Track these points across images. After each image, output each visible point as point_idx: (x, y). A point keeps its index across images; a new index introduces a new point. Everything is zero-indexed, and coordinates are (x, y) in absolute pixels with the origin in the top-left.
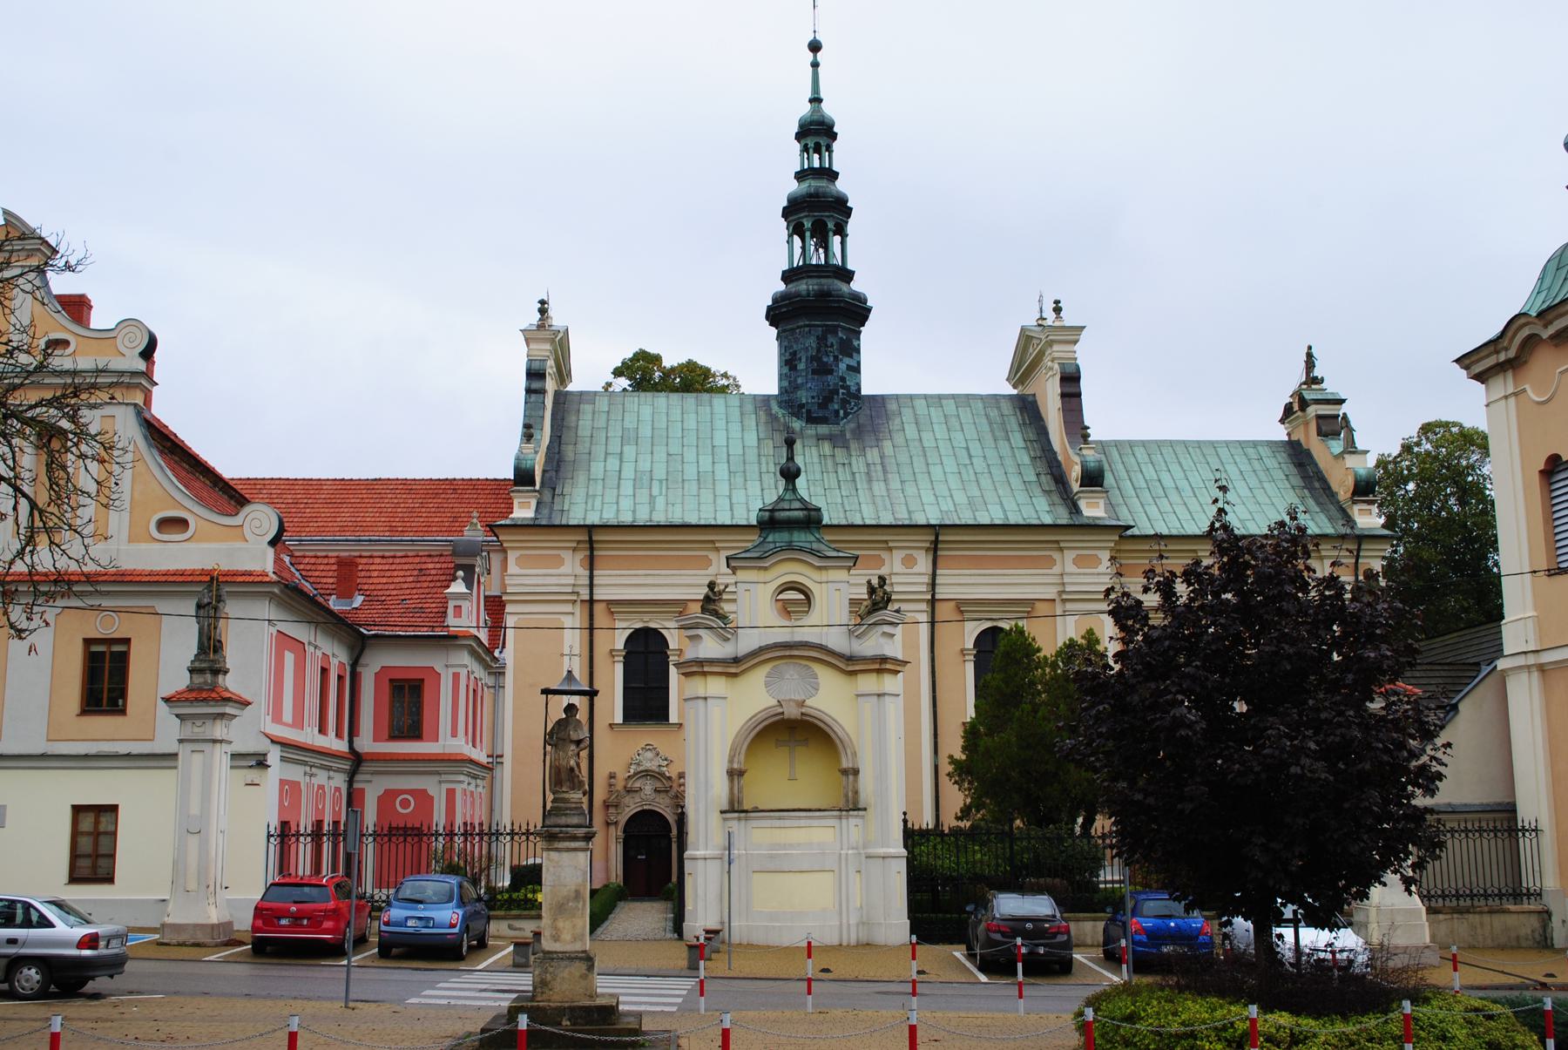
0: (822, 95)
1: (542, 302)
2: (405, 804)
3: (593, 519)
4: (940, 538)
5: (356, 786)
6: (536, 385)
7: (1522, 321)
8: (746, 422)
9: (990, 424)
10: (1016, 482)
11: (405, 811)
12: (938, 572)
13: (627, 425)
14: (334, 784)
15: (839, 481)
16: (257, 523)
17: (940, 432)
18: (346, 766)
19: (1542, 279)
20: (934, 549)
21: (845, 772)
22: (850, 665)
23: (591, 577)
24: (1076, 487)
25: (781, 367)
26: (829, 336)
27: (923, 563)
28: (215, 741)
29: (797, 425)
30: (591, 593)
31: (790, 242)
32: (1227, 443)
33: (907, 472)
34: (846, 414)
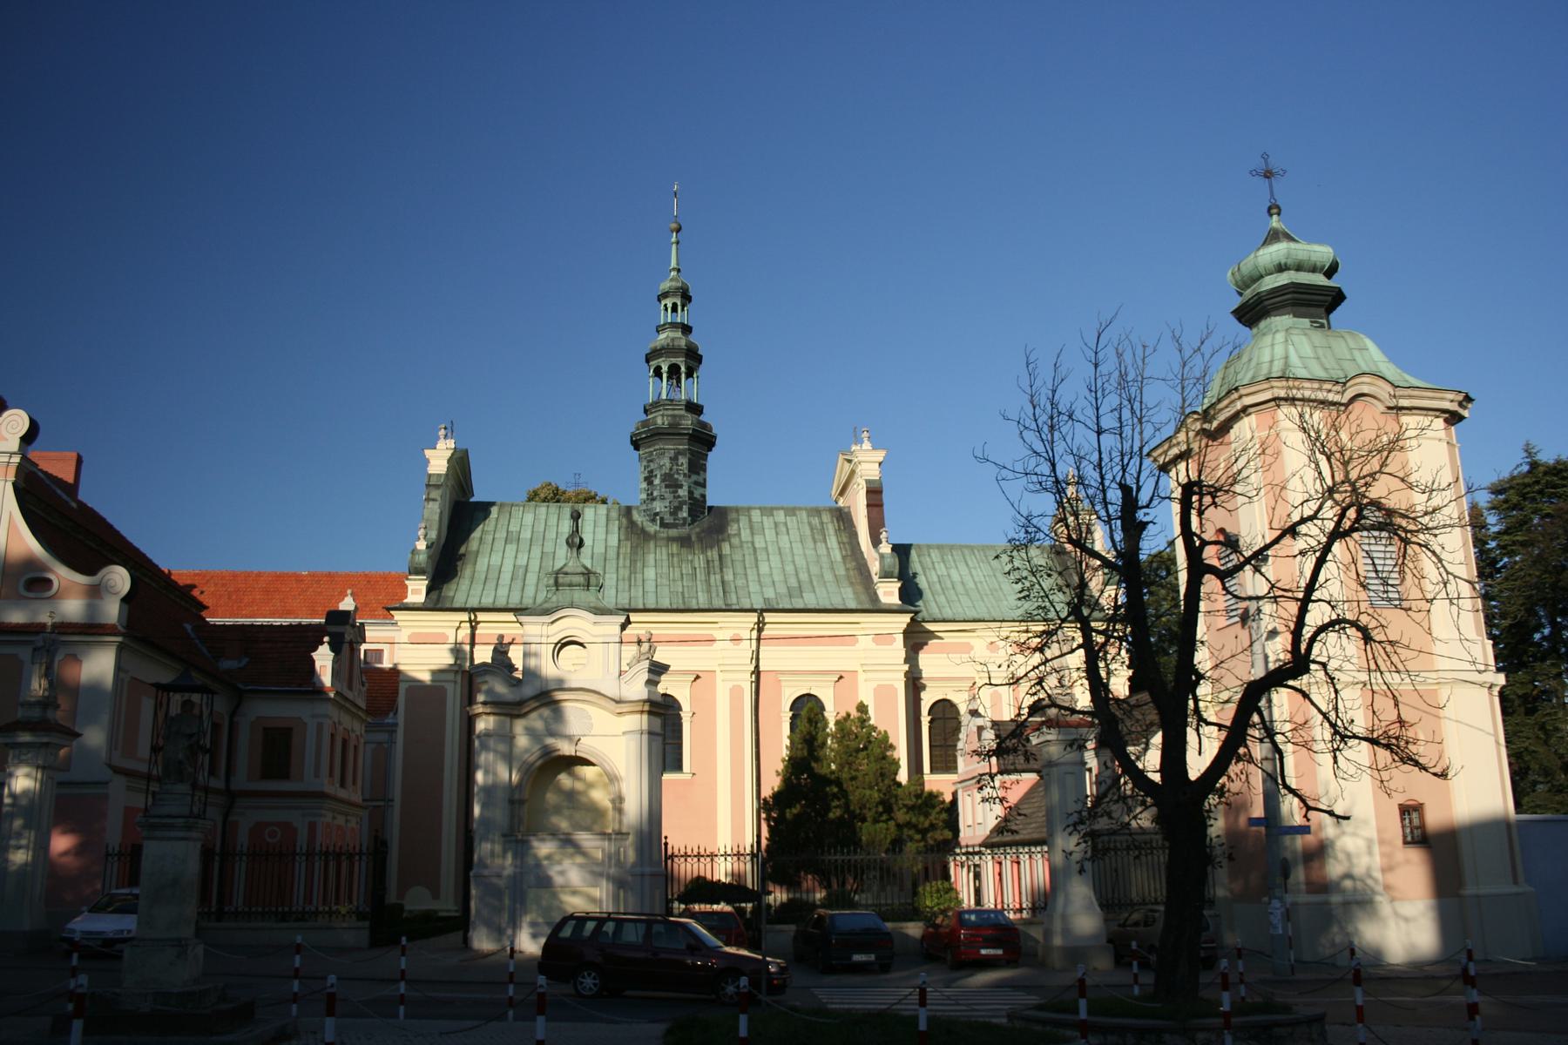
3: (473, 603)
9: (812, 529)
10: (828, 576)
13: (512, 528)
15: (682, 575)
24: (876, 579)
26: (680, 457)
29: (652, 528)
34: (693, 522)
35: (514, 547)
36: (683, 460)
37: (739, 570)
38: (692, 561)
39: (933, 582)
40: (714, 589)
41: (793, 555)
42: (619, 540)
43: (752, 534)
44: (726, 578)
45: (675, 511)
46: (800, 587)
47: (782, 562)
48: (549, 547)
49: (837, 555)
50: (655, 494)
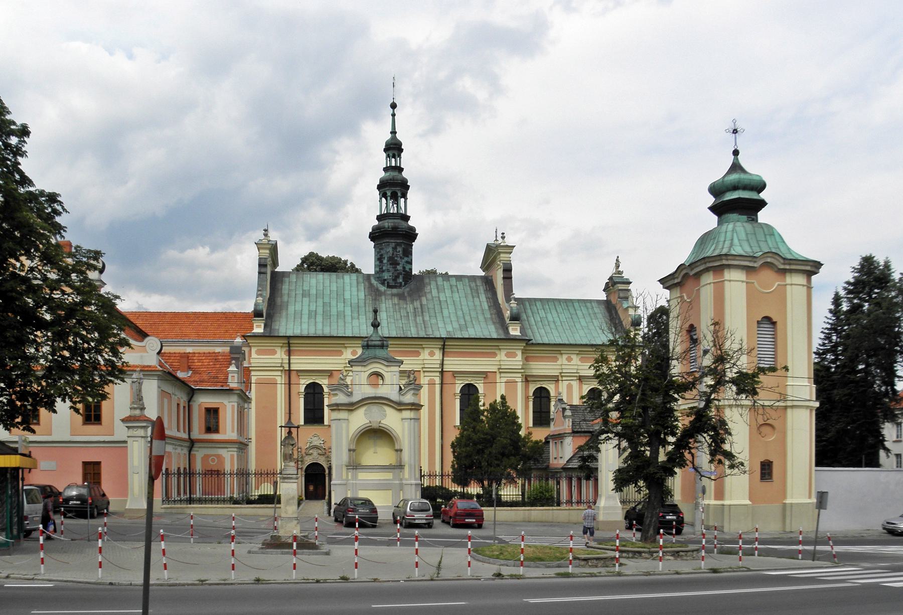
0: (397, 130)
1: (266, 230)
2: (213, 460)
4: (446, 343)
5: (192, 453)
8: (359, 287)
9: (471, 289)
10: (481, 318)
11: (213, 465)
12: (445, 359)
13: (305, 288)
14: (183, 452)
18: (187, 444)
20: (443, 348)
21: (397, 451)
22: (399, 406)
23: (289, 359)
24: (508, 321)
25: (375, 261)
27: (438, 355)
29: (382, 288)
30: (289, 367)
31: (380, 201)
33: (432, 311)
34: (405, 284)
36: (399, 249)
37: (432, 314)
38: (406, 308)
39: (538, 321)
41: (461, 305)
42: (365, 296)
43: (438, 293)
44: (425, 319)
45: (395, 280)
46: (466, 324)
47: (455, 309)
48: (327, 300)
50: (384, 268)
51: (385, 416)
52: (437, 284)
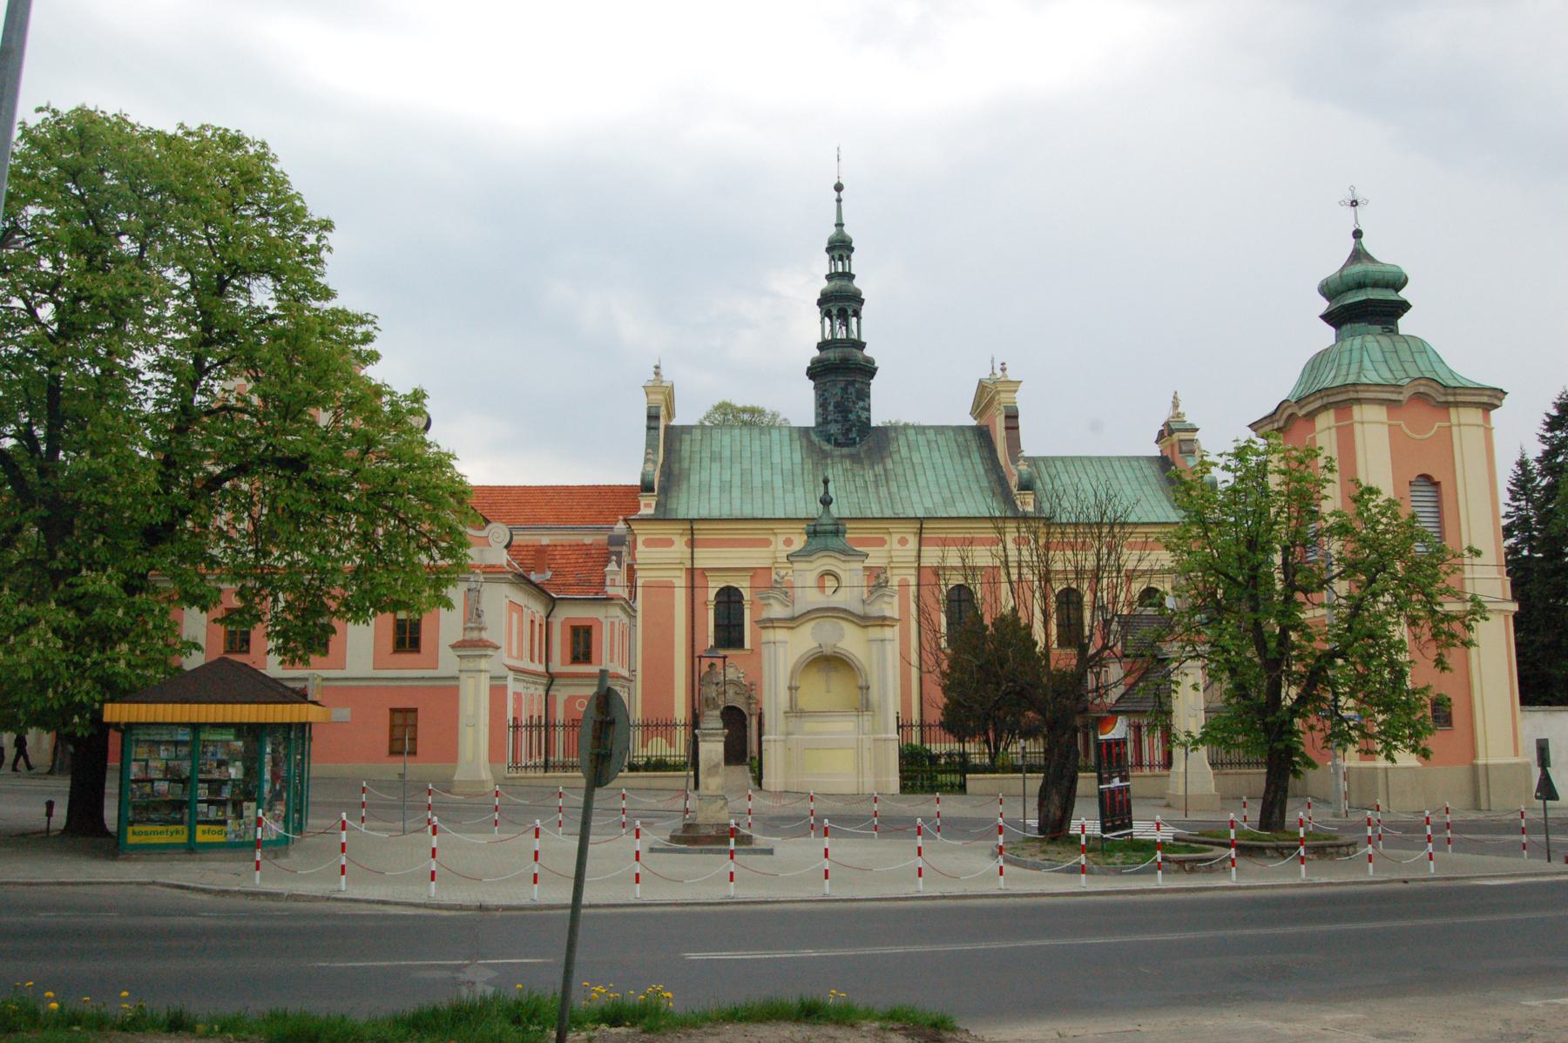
1: (657, 367)
3: (693, 514)
5: (551, 693)
6: (653, 425)
7: (1286, 405)
10: (975, 487)
12: (923, 548)
14: (538, 692)
16: (497, 535)
17: (925, 451)
18: (545, 681)
19: (1303, 374)
21: (861, 688)
22: (865, 621)
23: (692, 553)
24: (1015, 491)
25: (817, 408)
27: (913, 542)
28: (481, 671)
29: (827, 447)
31: (822, 321)
32: (1119, 458)
33: (901, 479)
34: (861, 440)
35: (718, 465)
38: (863, 476)
40: (884, 502)
41: (944, 470)
44: (892, 490)
47: (936, 476)
48: (746, 465)
49: (980, 470)
50: (829, 418)
51: (842, 636)
52: (907, 440)
